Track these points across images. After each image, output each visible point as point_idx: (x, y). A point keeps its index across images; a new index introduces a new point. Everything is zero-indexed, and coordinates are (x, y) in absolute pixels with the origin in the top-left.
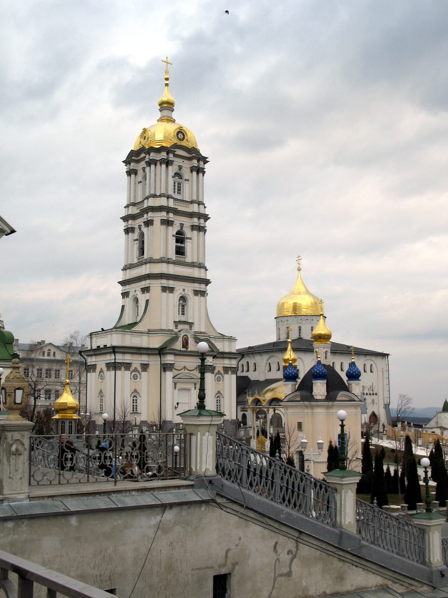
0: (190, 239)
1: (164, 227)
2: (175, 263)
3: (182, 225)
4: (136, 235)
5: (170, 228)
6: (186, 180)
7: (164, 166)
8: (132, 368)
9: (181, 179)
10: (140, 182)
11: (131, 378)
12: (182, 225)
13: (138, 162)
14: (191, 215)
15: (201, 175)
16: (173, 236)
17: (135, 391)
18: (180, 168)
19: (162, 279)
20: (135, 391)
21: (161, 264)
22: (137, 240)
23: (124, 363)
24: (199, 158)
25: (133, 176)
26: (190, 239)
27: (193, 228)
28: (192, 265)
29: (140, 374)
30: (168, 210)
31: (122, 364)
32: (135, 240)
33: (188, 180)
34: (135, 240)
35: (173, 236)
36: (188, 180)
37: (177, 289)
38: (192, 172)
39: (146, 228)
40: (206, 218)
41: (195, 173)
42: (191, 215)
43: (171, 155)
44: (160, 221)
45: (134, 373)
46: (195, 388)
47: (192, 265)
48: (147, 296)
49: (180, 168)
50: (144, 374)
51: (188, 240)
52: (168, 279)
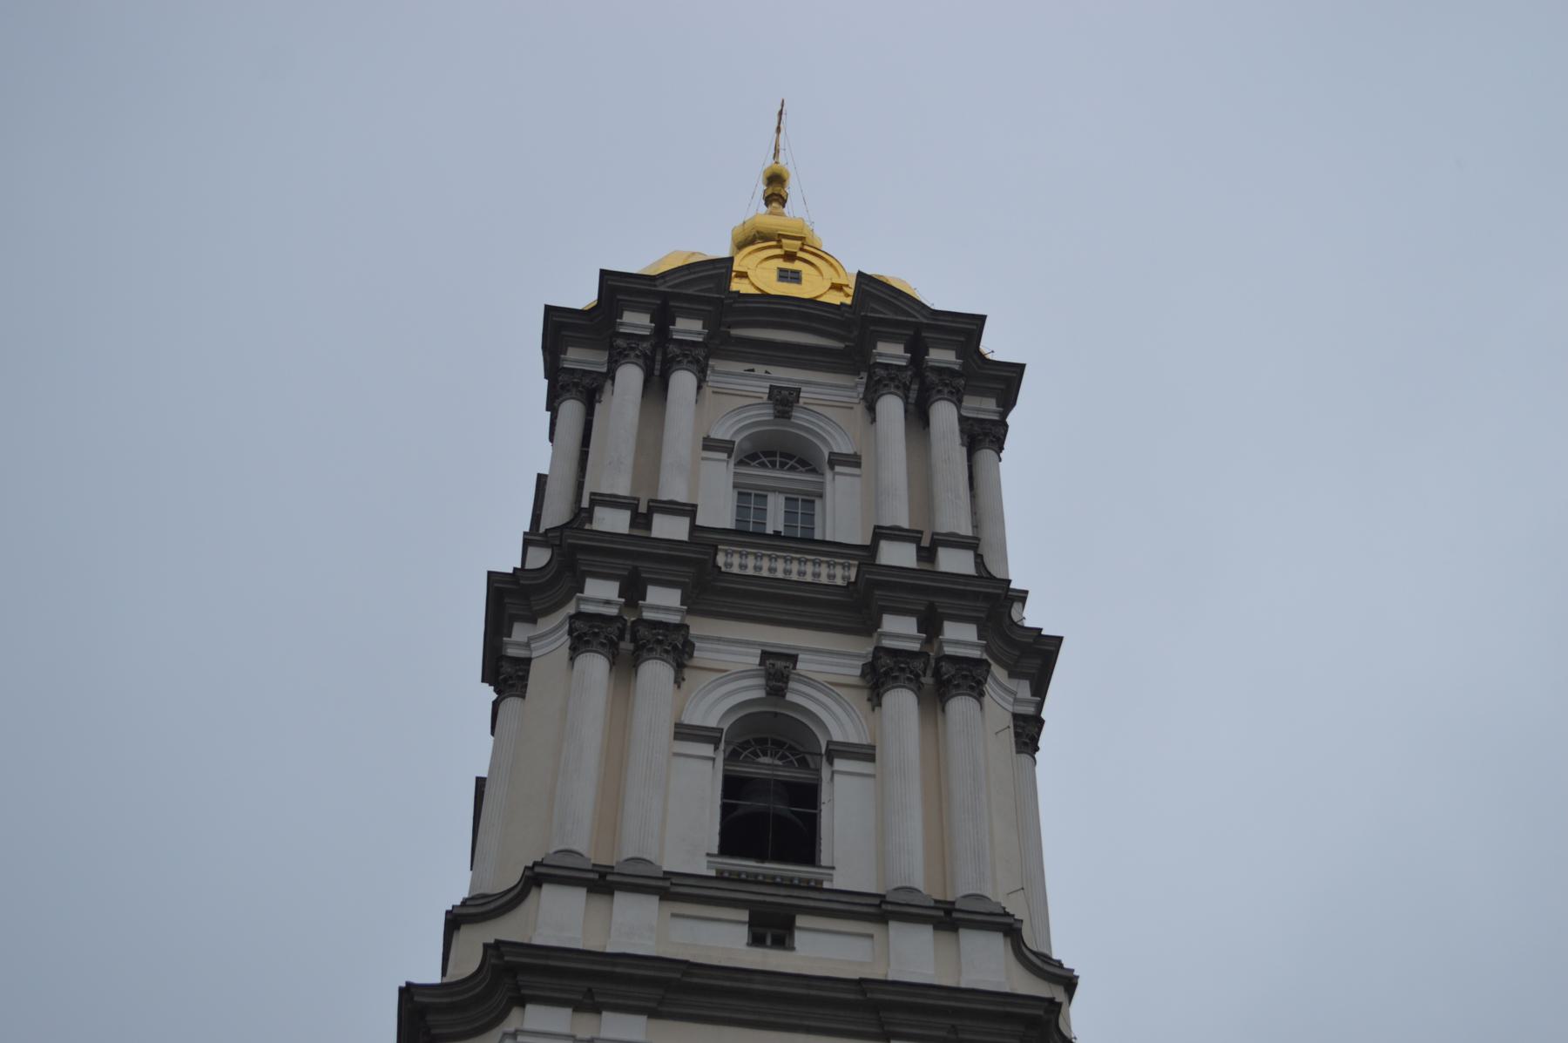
0: (866, 753)
1: (595, 666)
2: (669, 888)
3: (778, 670)
5: (655, 673)
6: (836, 460)
7: (630, 377)
9: (814, 471)
12: (778, 670)
14: (858, 603)
15: (944, 415)
16: (684, 732)
18: (784, 401)
19: (522, 1002)
21: (534, 892)
24: (918, 327)
26: (866, 753)
27: (880, 675)
28: (880, 910)
30: (636, 562)
33: (853, 461)
35: (684, 732)
36: (853, 461)
40: (1036, 657)
41: (892, 408)
42: (858, 603)
43: (688, 328)
47: (880, 910)
49: (784, 401)
51: (839, 764)
52: (588, 1005)
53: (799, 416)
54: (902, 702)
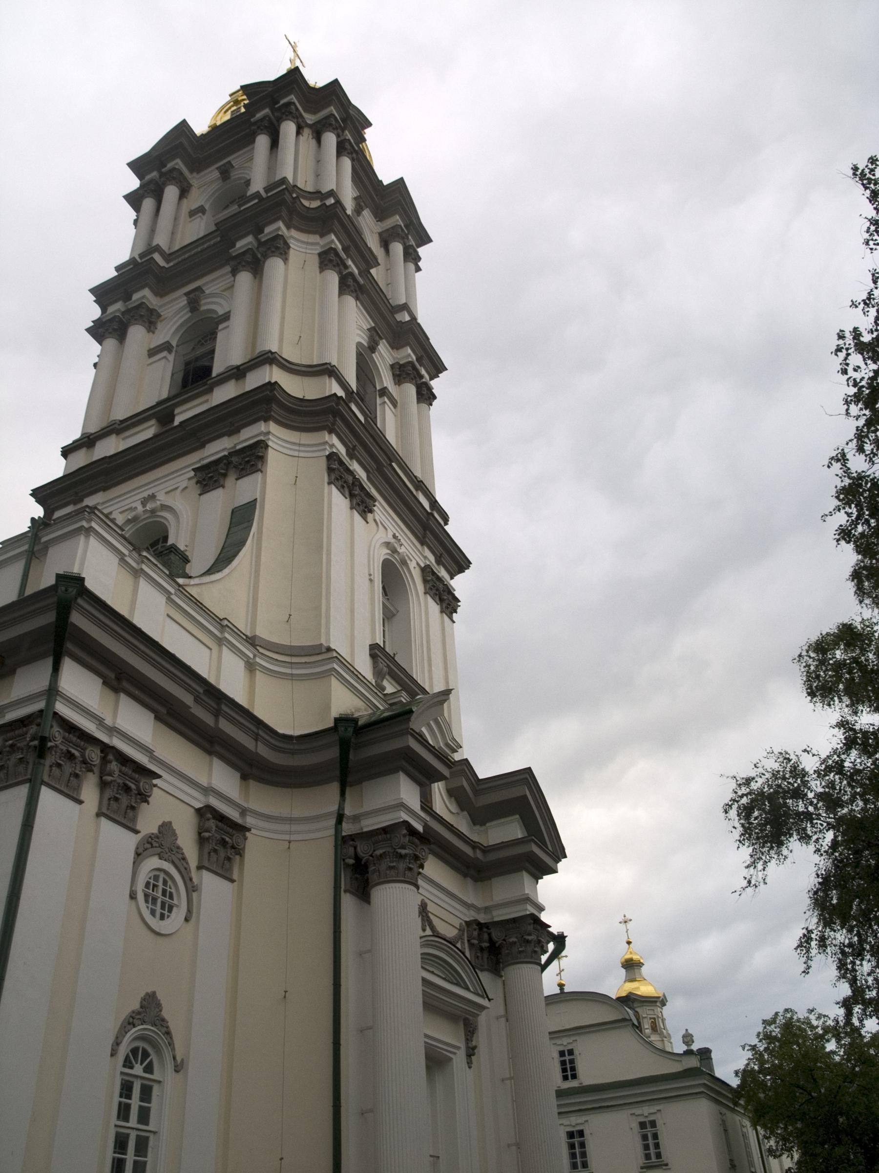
4: (166, 332)
7: (330, 140)
8: (149, 820)
10: (201, 210)
11: (133, 896)
13: (197, 166)
17: (149, 1010)
20: (149, 1010)
22: (166, 347)
23: (106, 749)
24: (411, 222)
25: (171, 192)
26: (394, 404)
27: (402, 373)
29: (192, 888)
31: (94, 755)
32: (152, 352)
34: (152, 352)
37: (377, 518)
38: (385, 244)
39: (244, 278)
44: (316, 260)
45: (153, 863)
46: (471, 1052)
48: (241, 490)
50: (211, 884)
53: (360, 219)
54: (410, 390)
